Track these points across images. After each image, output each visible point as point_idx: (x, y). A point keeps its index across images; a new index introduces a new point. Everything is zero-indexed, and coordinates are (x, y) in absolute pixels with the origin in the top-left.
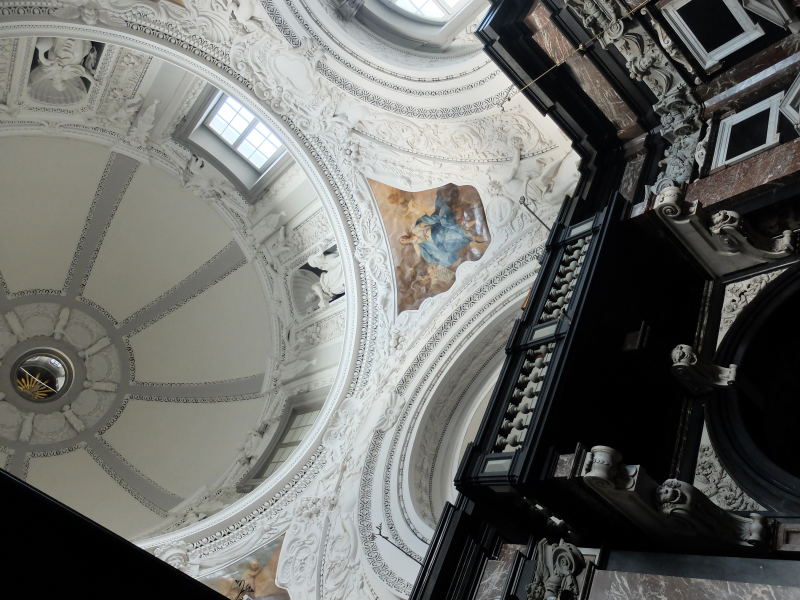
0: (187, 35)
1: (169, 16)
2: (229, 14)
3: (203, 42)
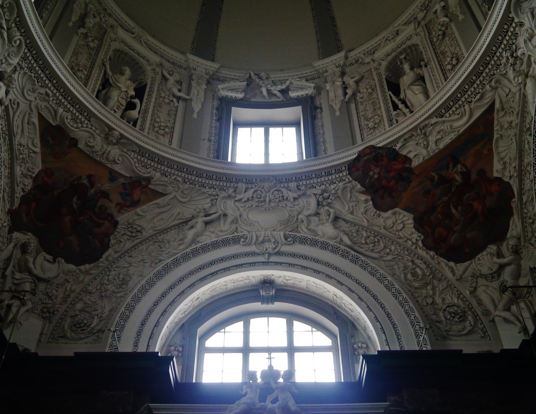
0: (48, 91)
1: (56, 112)
2: (10, 96)
3: (38, 78)
